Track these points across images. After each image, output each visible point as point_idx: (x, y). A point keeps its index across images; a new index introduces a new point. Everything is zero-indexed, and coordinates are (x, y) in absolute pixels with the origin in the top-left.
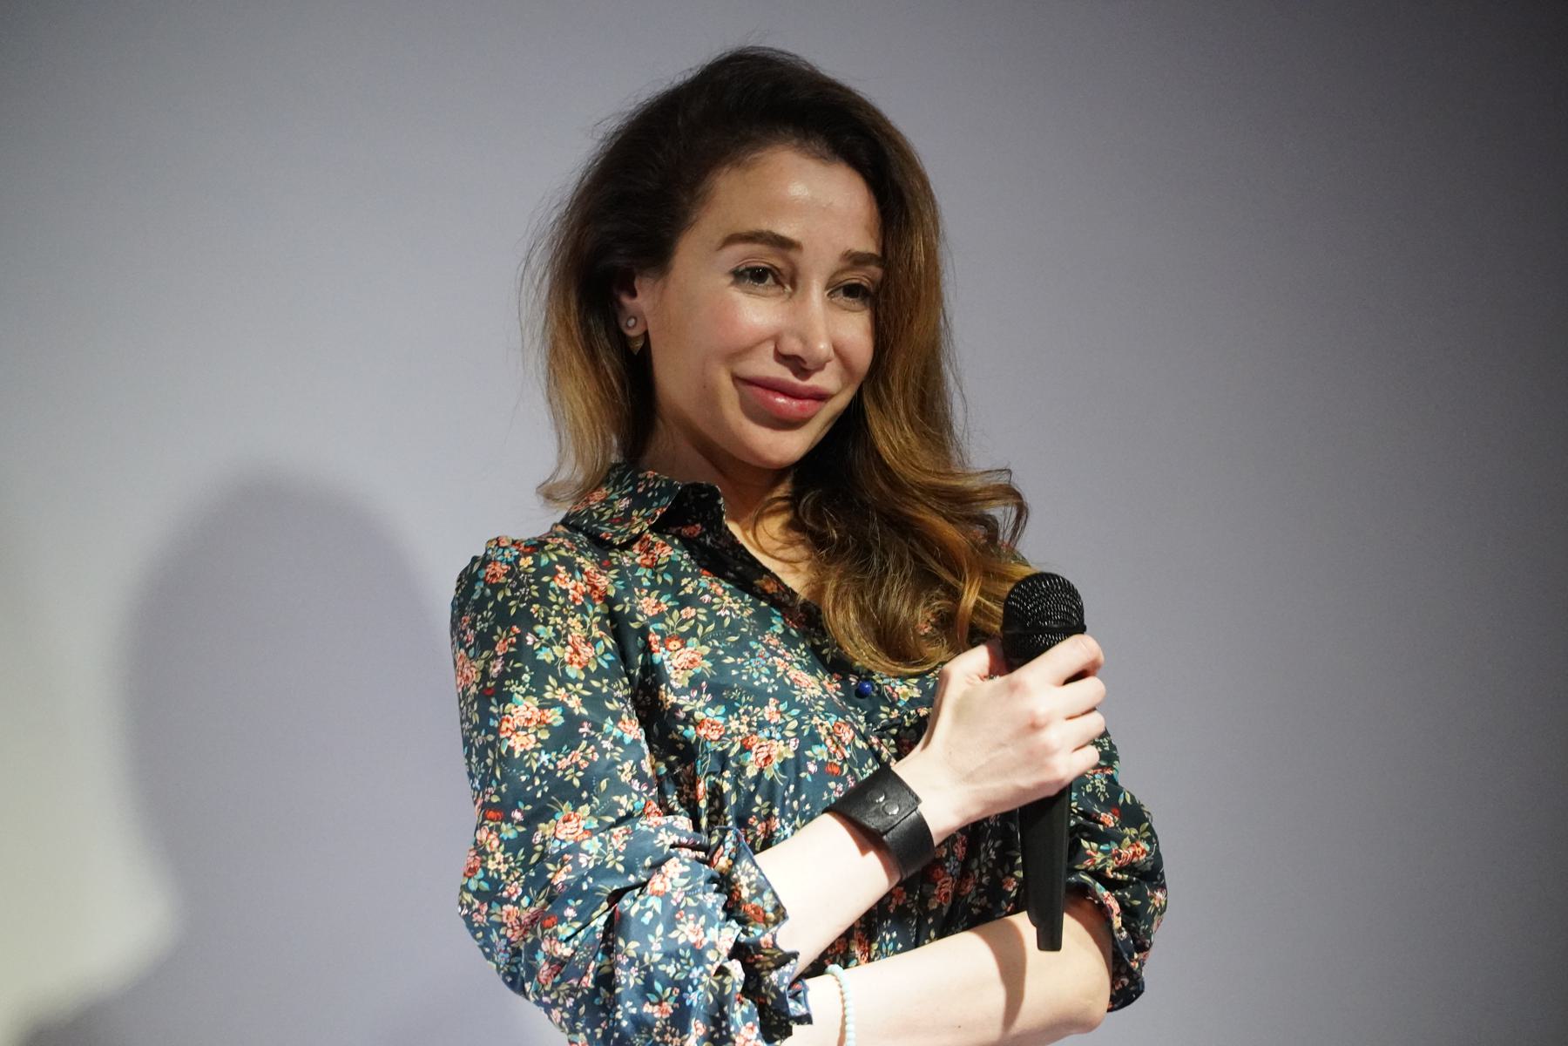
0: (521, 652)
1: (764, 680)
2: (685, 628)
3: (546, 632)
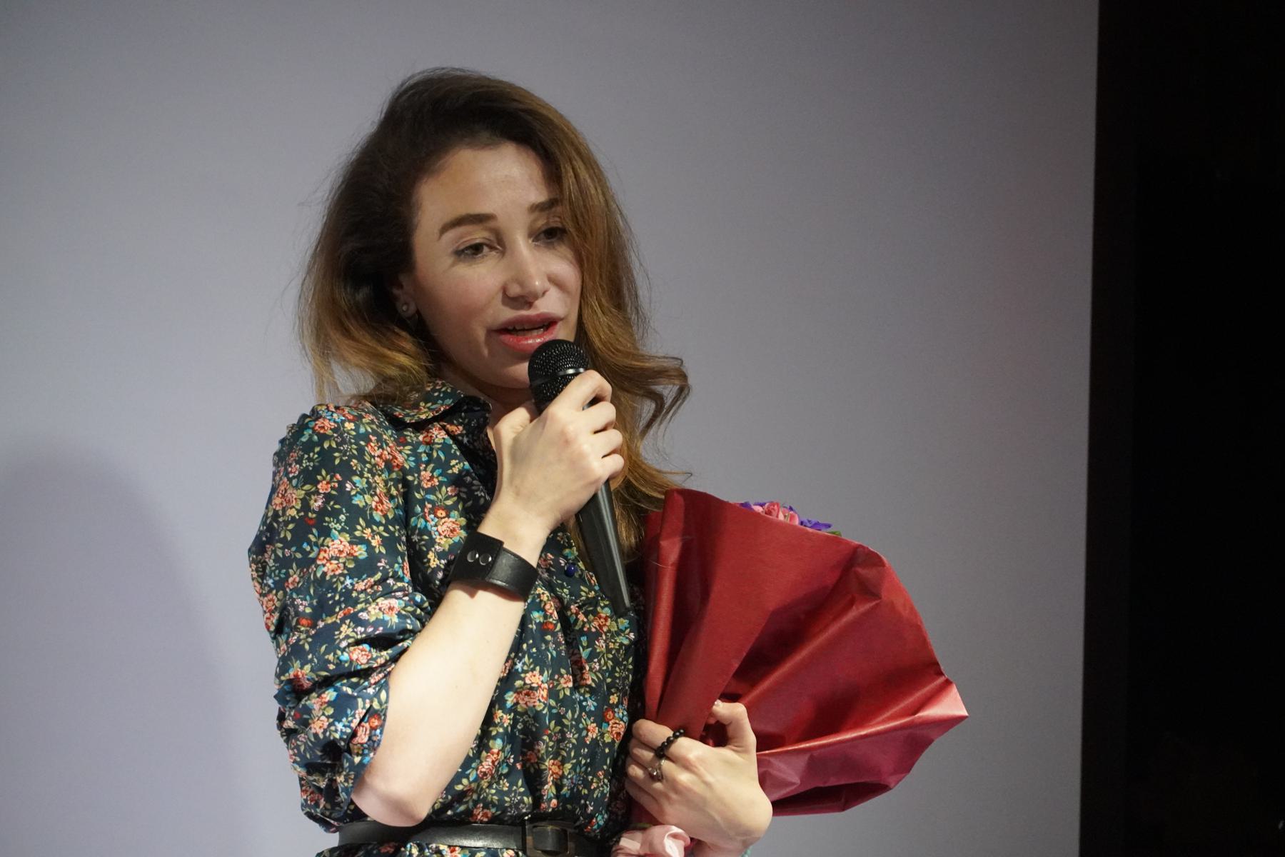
0: (342, 497)
3: (360, 483)
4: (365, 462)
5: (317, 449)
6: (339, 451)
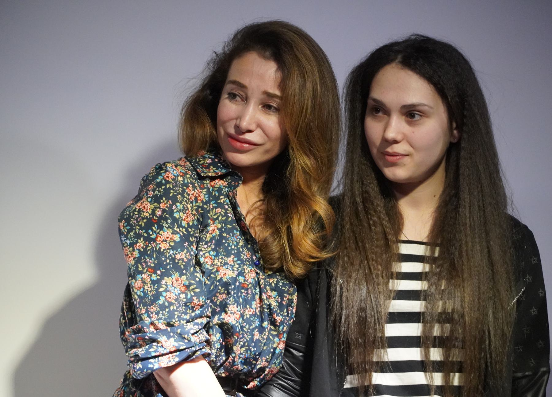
1: (233, 247)
2: (215, 217)
3: (180, 206)
4: (184, 197)
5: (163, 187)
6: (173, 190)
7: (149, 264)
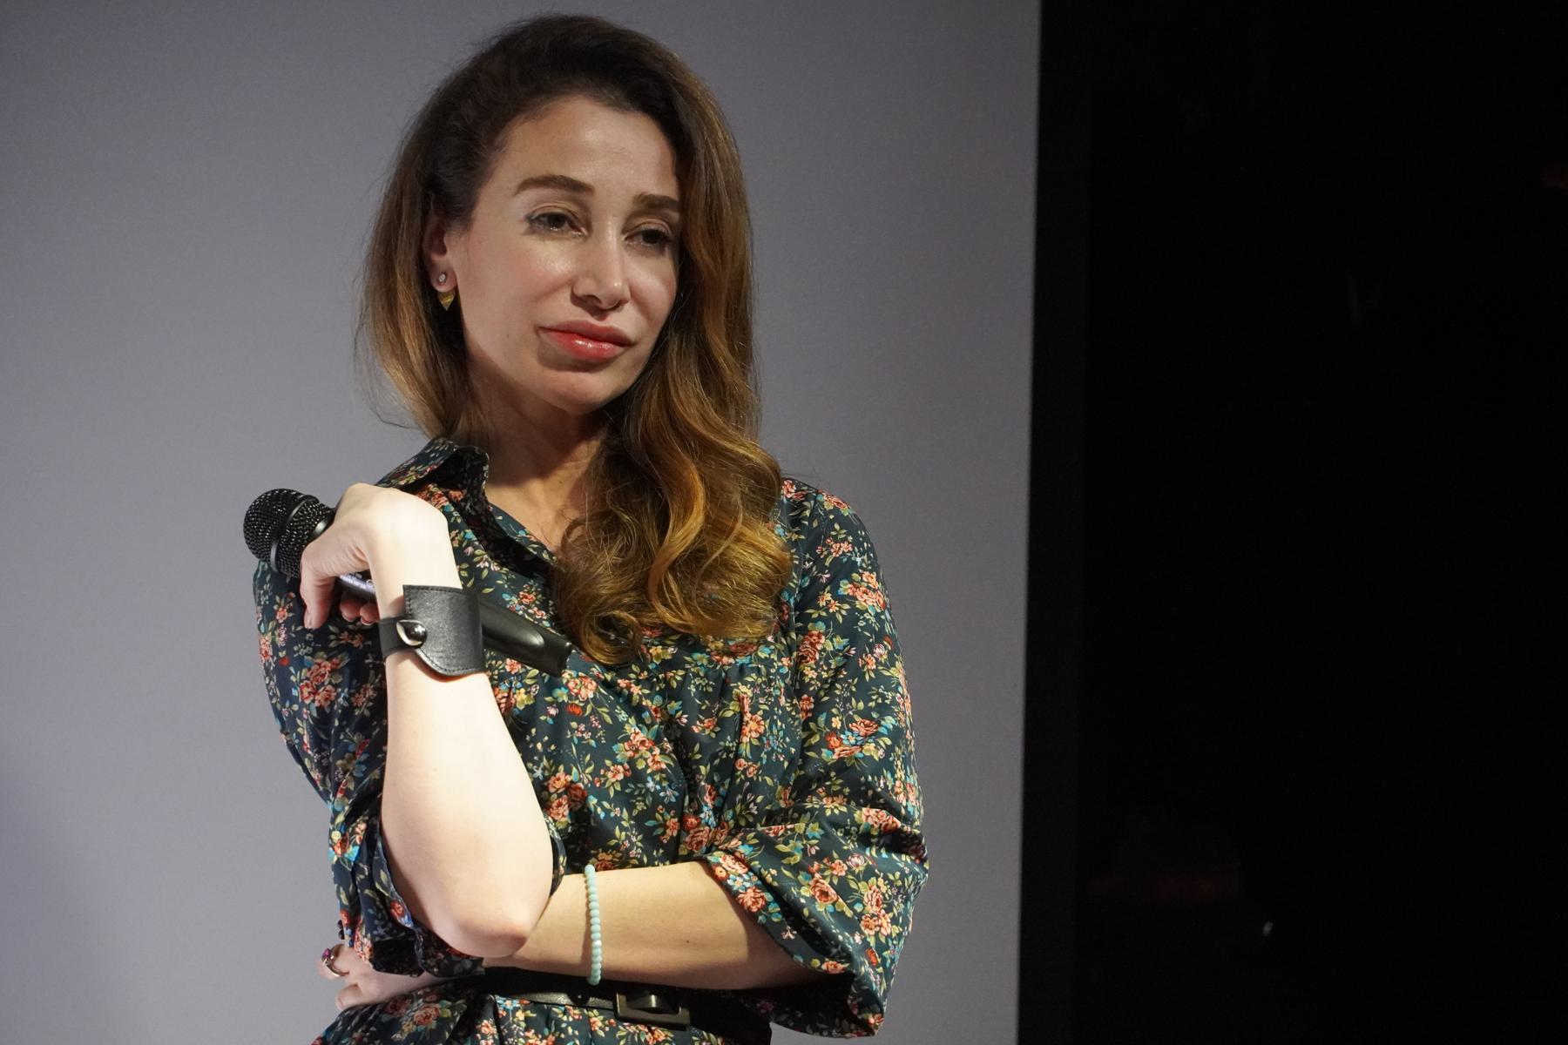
7: (582, 727)
